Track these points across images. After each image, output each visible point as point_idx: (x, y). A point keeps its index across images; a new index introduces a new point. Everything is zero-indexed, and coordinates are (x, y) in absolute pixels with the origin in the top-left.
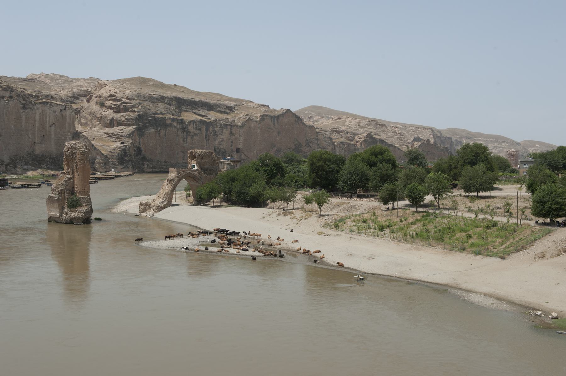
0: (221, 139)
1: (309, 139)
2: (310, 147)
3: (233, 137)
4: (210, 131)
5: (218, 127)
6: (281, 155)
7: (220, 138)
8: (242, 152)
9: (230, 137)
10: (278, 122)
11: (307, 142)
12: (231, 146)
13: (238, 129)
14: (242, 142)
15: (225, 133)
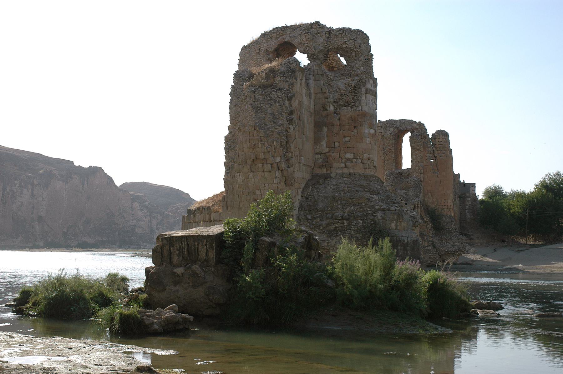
0: (20, 203)
1: (123, 207)
2: (124, 218)
3: (35, 201)
4: (8, 190)
5: (18, 185)
6: (91, 227)
7: (19, 201)
8: (45, 222)
9: (31, 201)
10: (88, 183)
11: (120, 211)
12: (33, 213)
13: (41, 189)
14: (45, 207)
15: (25, 194)
